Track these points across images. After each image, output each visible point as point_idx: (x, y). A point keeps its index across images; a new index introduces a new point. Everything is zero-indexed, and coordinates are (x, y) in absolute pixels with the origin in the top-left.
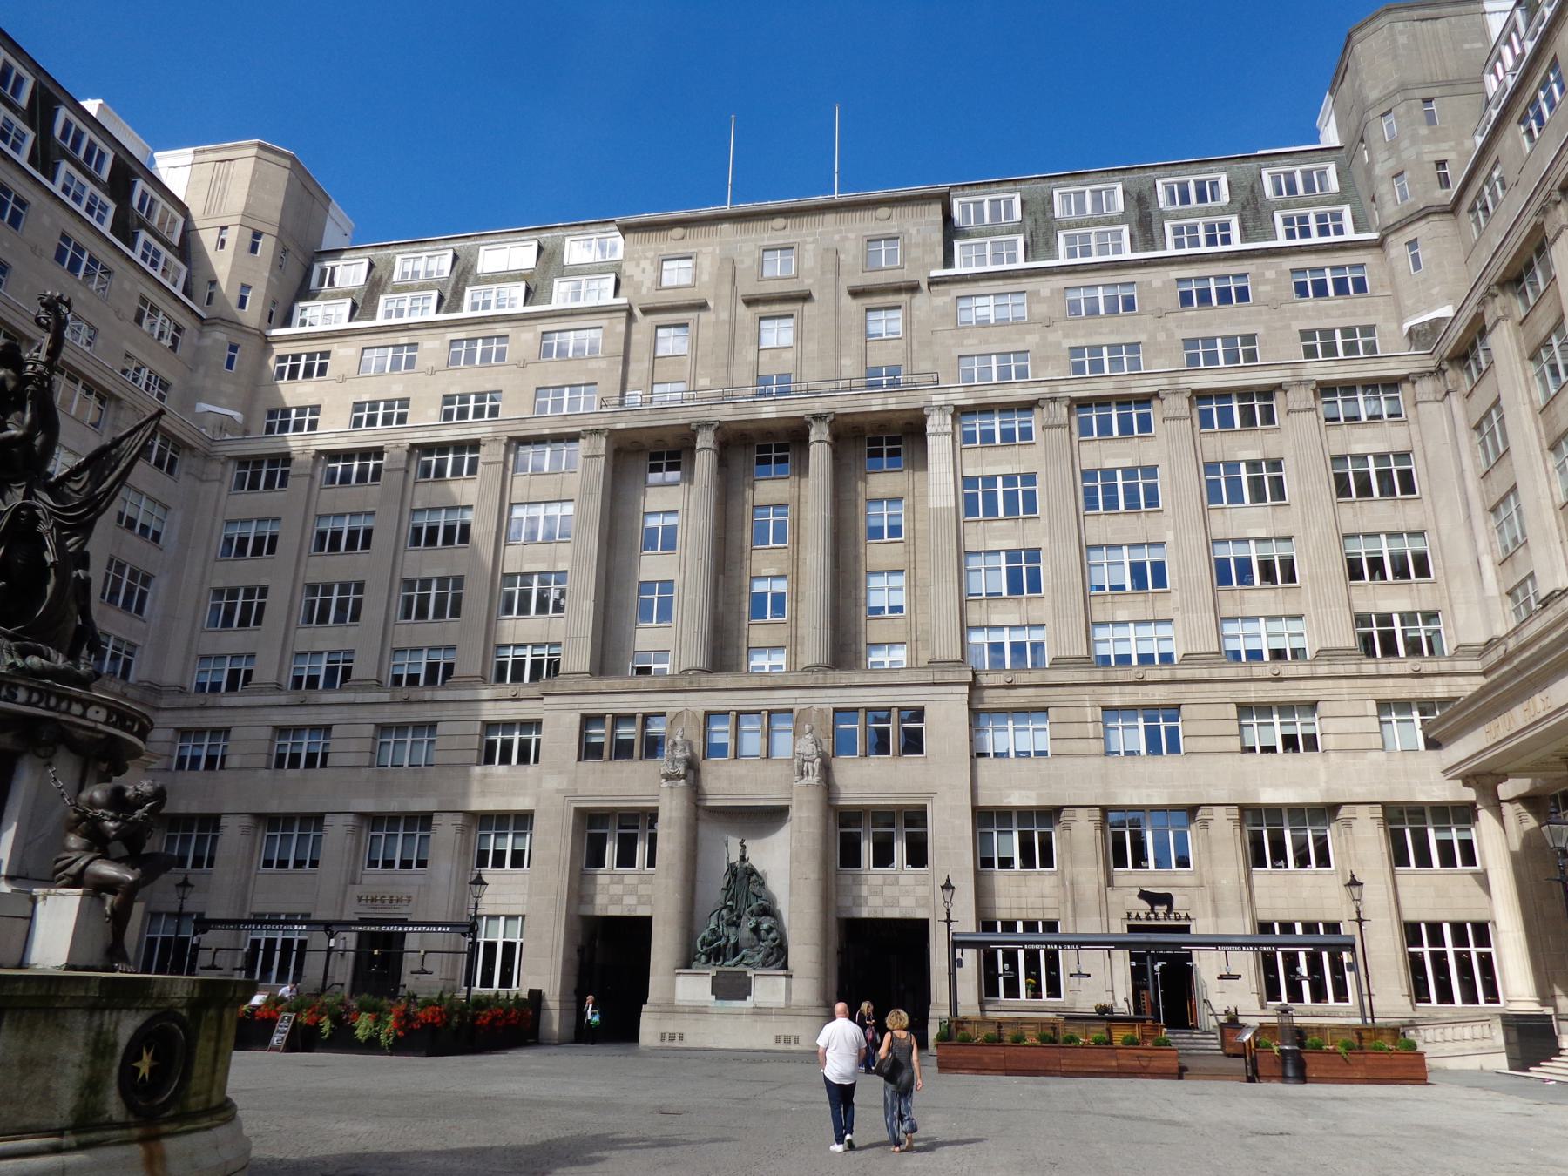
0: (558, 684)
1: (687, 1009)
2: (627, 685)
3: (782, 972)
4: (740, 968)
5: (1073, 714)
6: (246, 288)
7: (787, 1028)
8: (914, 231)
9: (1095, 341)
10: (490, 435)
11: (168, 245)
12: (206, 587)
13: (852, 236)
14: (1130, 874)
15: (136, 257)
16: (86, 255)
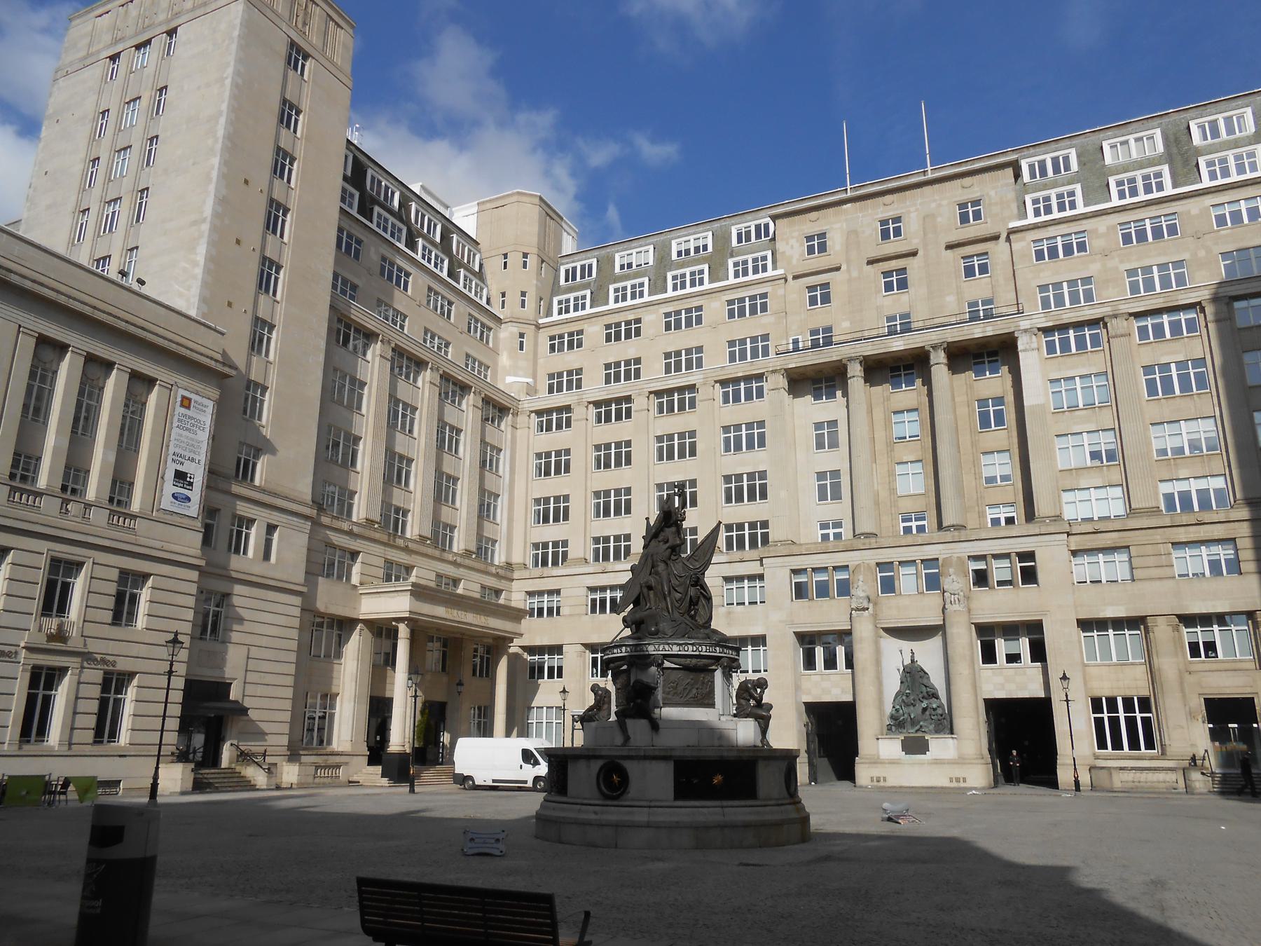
0: (770, 550)
1: (887, 761)
2: (819, 548)
3: (950, 736)
4: (920, 734)
5: (1149, 550)
6: (523, 294)
7: (958, 772)
8: (992, 193)
9: (1146, 263)
10: (701, 380)
11: (390, 211)
12: (530, 498)
13: (945, 202)
14: (1203, 662)
15: (374, 226)
16: (345, 233)
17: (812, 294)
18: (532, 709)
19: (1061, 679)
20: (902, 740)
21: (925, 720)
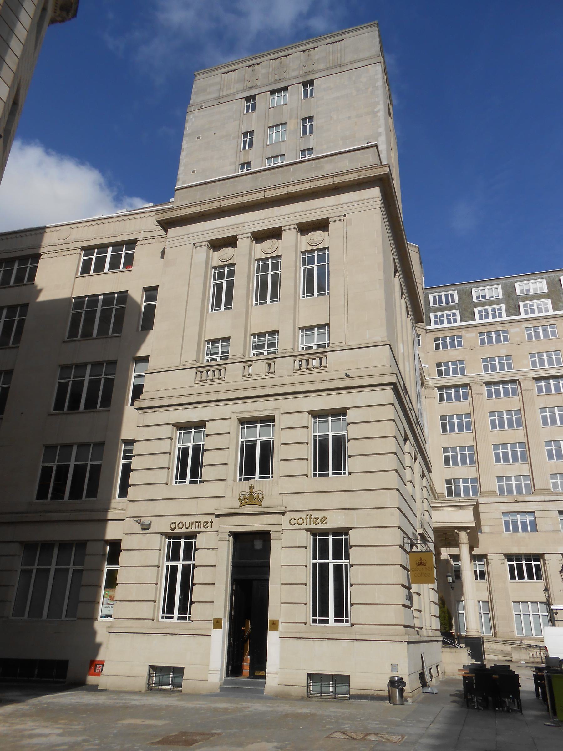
17: (459, 340)
18: (461, 603)
19: (543, 590)
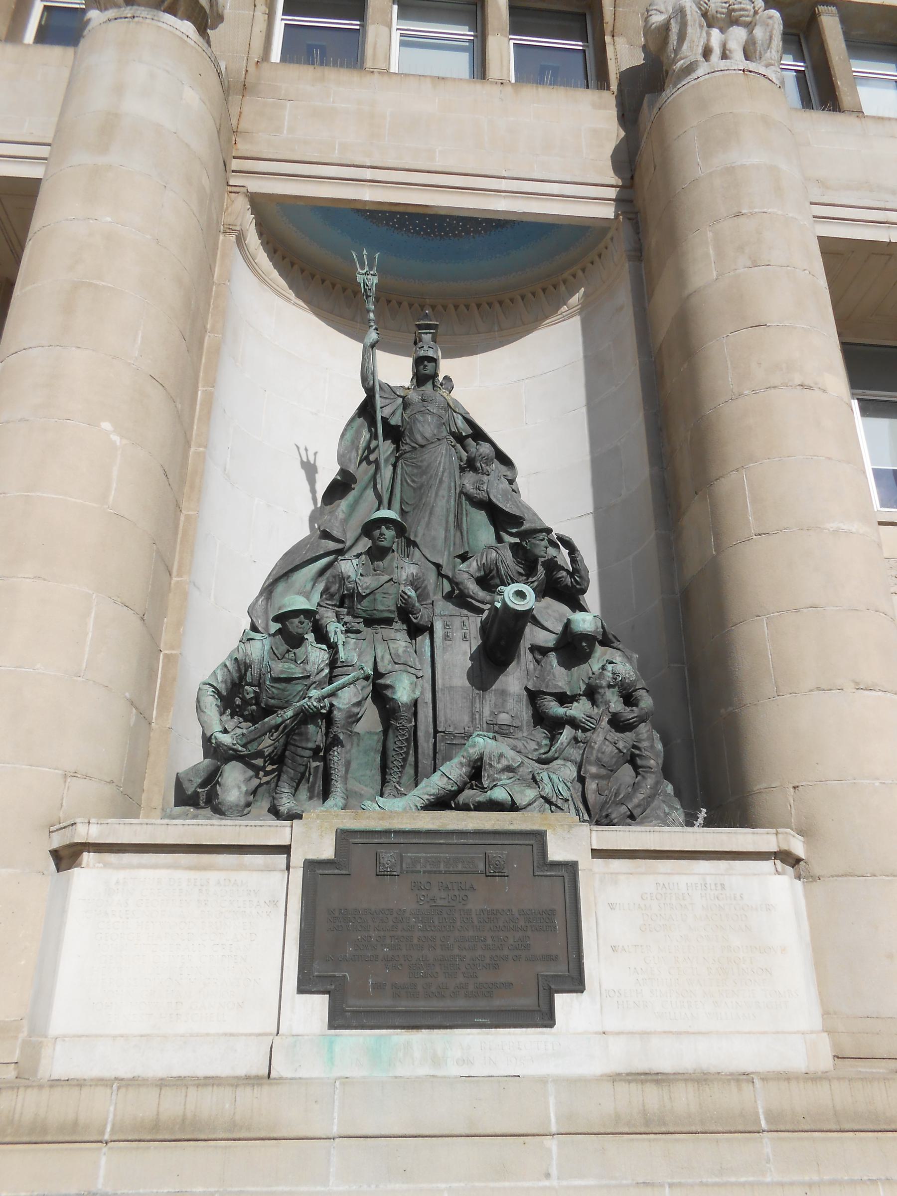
20: (311, 866)
21: (500, 731)
